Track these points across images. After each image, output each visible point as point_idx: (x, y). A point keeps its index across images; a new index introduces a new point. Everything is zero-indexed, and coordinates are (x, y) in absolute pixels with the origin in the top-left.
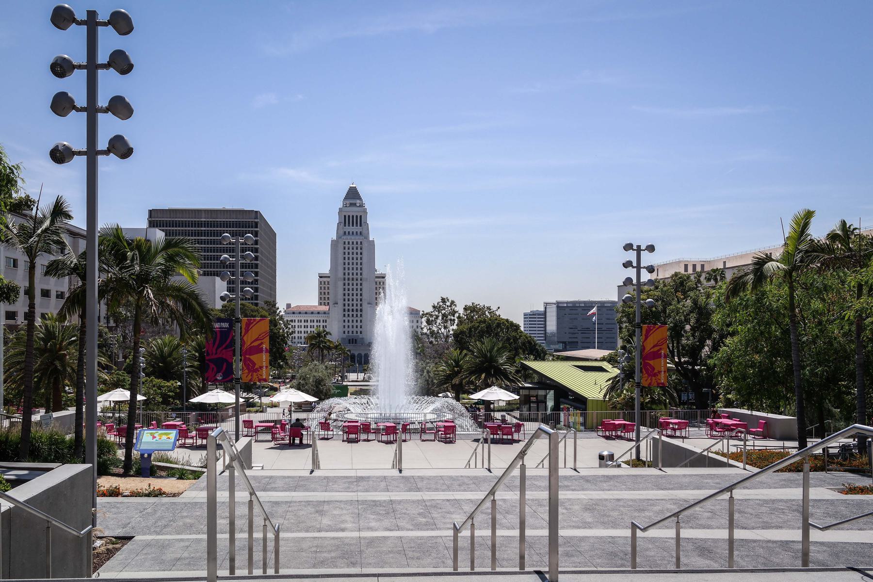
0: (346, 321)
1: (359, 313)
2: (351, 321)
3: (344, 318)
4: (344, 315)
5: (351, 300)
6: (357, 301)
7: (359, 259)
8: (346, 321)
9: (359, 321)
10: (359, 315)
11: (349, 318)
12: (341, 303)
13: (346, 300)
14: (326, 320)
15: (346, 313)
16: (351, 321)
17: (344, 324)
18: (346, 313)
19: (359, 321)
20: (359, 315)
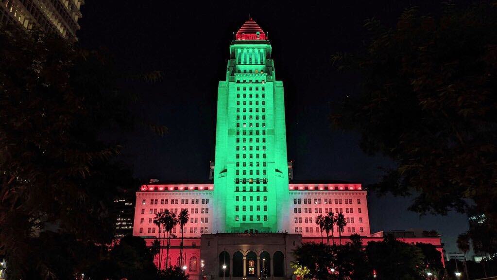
0: (241, 198)
1: (261, 186)
2: (248, 199)
3: (237, 194)
4: (237, 190)
5: (248, 164)
6: (258, 165)
7: (260, 103)
8: (241, 198)
9: (262, 198)
10: (262, 189)
11: (244, 194)
12: (232, 169)
13: (241, 164)
14: (207, 200)
15: (241, 185)
16: (248, 199)
17: (237, 203)
18: (241, 185)
19: (262, 198)
20: (262, 189)
